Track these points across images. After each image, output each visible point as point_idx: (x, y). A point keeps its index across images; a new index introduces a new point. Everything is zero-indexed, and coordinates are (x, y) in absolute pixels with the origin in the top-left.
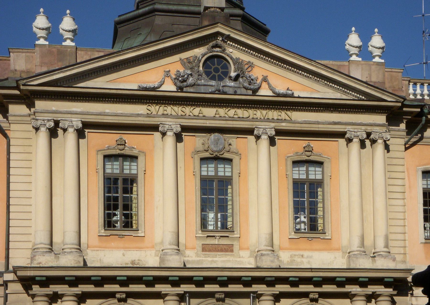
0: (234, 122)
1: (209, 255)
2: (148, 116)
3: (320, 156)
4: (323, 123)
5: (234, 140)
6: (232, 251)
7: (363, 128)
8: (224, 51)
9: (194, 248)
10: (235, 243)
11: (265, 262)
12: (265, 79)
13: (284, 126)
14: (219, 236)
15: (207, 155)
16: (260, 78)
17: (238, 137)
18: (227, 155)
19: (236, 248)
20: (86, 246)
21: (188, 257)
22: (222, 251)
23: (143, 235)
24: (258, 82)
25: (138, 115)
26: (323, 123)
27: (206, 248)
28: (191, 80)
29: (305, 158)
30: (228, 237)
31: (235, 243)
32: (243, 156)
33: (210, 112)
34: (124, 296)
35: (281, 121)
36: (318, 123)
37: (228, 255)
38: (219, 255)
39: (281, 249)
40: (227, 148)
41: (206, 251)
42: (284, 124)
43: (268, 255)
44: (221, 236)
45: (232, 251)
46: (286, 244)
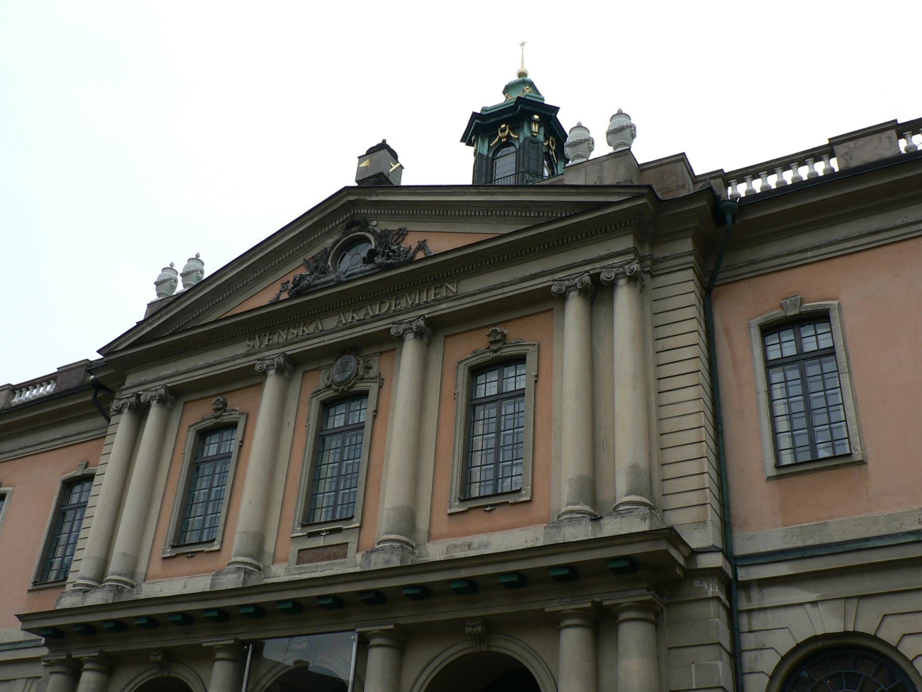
0: (365, 327)
1: (306, 568)
2: (247, 355)
3: (517, 344)
4: (511, 283)
5: (376, 358)
6: (345, 556)
7: (588, 268)
8: (365, 225)
9: (286, 560)
10: (352, 540)
11: (375, 564)
12: (422, 246)
13: (445, 308)
14: (326, 531)
15: (328, 394)
16: (414, 246)
17: (381, 353)
18: (360, 386)
19: (352, 547)
20: (143, 577)
21: (274, 577)
22: (328, 558)
23: (217, 548)
24: (412, 252)
25: (235, 358)
26: (511, 283)
27: (304, 556)
28: (304, 283)
29: (490, 355)
30: (339, 530)
31: (352, 540)
32: (386, 382)
33: (330, 323)
34: (159, 658)
35: (437, 302)
36: (503, 285)
37: (338, 564)
38: (322, 566)
39: (430, 537)
40: (361, 373)
41: (303, 563)
42: (443, 306)
43: (383, 549)
44: (332, 532)
45: (345, 556)
46: (442, 524)
